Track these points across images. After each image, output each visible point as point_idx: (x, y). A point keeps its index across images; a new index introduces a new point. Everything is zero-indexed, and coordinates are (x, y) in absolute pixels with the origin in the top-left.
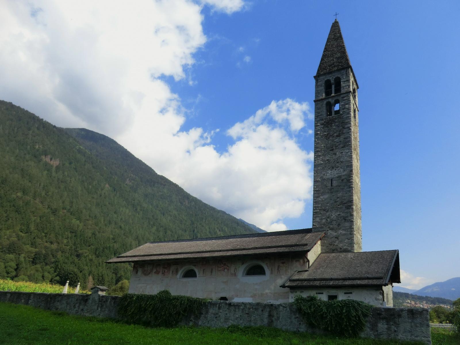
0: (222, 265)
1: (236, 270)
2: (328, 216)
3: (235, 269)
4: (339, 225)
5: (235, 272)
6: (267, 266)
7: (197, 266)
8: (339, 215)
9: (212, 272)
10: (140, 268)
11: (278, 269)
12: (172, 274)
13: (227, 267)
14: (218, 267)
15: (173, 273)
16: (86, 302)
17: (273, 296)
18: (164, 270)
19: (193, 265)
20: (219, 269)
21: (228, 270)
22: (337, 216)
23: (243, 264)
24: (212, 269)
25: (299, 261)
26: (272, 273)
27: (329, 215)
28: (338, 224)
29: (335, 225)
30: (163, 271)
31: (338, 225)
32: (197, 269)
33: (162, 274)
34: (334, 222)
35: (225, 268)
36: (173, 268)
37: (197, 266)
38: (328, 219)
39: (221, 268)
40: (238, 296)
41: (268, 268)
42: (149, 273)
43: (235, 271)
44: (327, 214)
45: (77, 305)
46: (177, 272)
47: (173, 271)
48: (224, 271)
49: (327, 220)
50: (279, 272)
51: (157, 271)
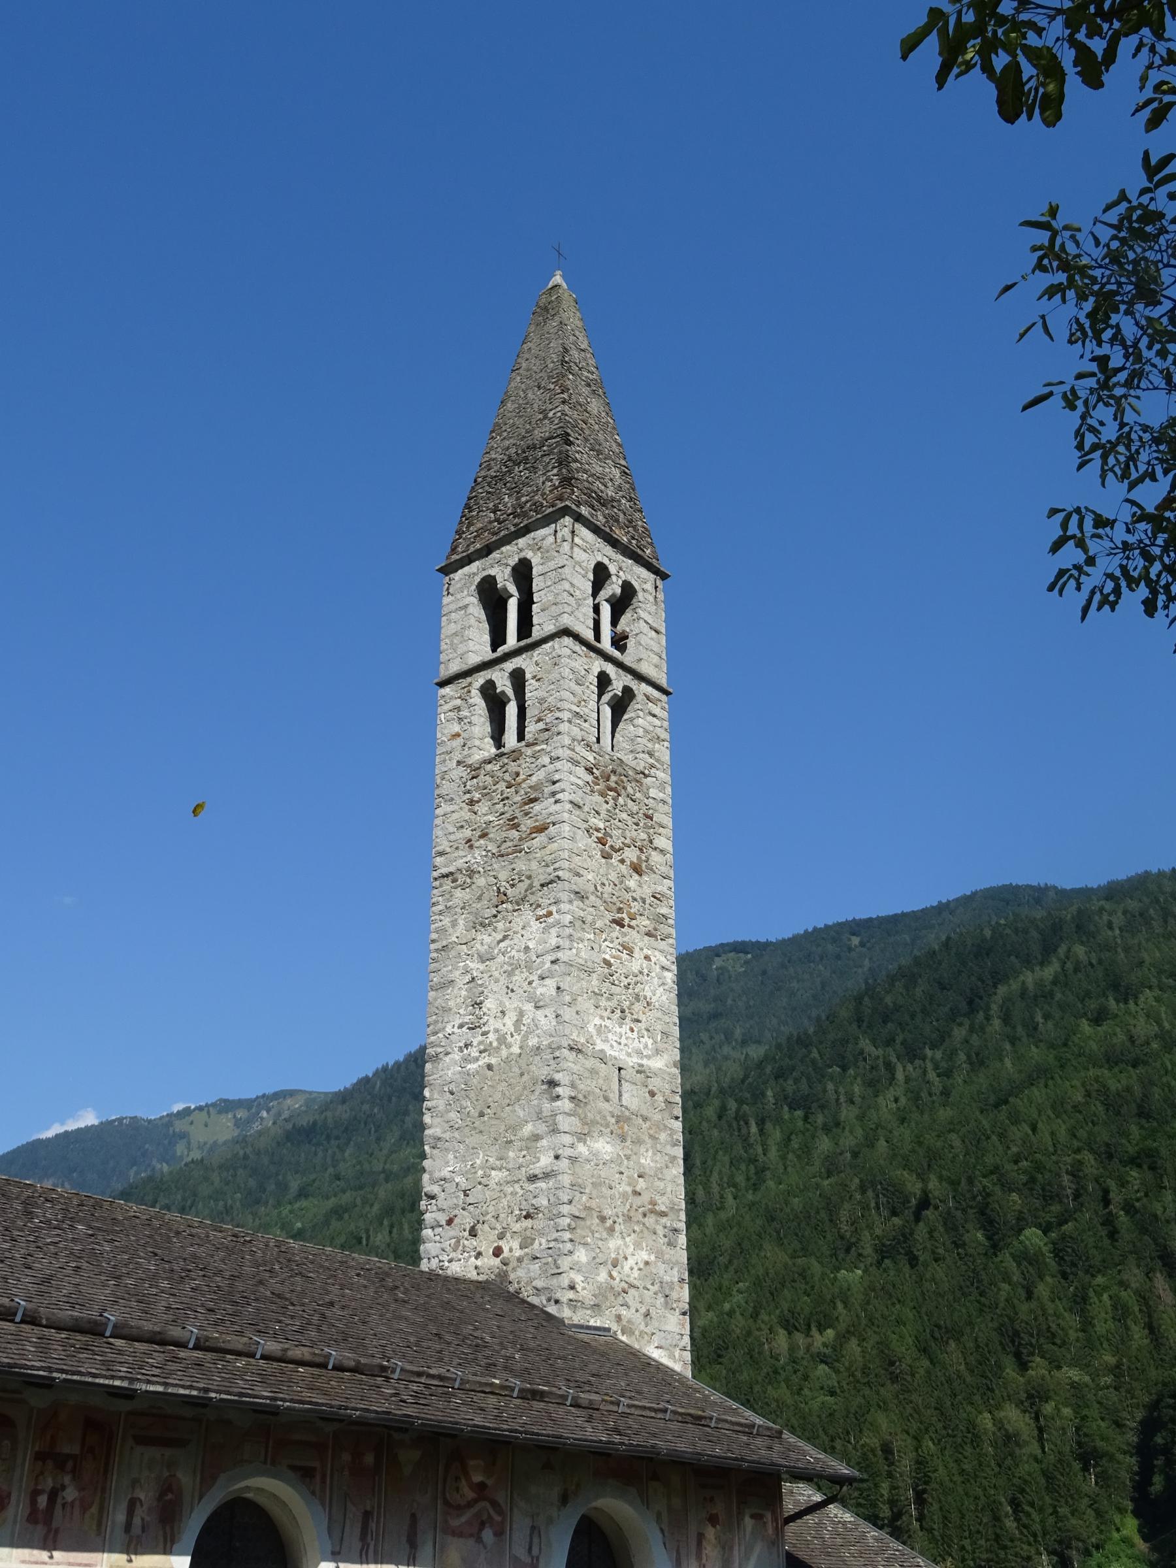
1: (536, 1540)
3: (533, 1528)
6: (662, 1531)
19: (293, 1468)
21: (499, 1534)
22: (640, 1269)
23: (564, 1499)
32: (323, 1505)
39: (463, 1519)
44: (614, 1243)
48: (479, 1540)
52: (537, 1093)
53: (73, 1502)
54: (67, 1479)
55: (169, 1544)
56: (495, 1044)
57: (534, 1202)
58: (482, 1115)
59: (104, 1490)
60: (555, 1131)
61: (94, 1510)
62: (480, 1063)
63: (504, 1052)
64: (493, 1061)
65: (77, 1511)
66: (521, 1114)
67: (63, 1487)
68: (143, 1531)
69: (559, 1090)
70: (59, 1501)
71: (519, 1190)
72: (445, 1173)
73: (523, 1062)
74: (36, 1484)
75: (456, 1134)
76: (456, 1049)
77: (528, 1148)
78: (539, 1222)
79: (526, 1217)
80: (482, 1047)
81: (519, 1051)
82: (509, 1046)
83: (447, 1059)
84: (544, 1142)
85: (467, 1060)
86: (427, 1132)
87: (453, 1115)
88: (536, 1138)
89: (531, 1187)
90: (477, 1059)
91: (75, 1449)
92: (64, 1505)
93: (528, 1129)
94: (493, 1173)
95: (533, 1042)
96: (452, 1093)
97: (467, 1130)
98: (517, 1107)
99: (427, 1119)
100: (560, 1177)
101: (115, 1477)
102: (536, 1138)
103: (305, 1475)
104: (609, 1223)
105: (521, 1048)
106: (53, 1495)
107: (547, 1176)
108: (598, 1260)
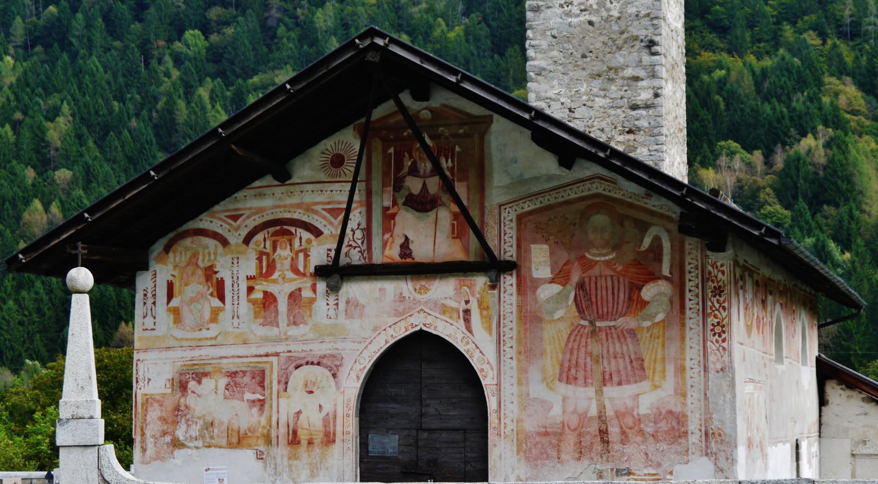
52: (636, 48)
56: (595, 7)
57: (636, 123)
58: (584, 56)
60: (653, 75)
62: (582, 18)
63: (604, 14)
64: (594, 19)
66: (621, 60)
69: (656, 48)
71: (621, 113)
72: (551, 94)
73: (622, 23)
75: (560, 68)
76: (557, 5)
77: (628, 85)
78: (640, 137)
79: (628, 132)
80: (583, 7)
81: (617, 15)
82: (609, 10)
83: (549, 11)
84: (643, 83)
85: (569, 14)
86: (528, 63)
87: (555, 53)
88: (637, 79)
89: (634, 113)
90: (578, 16)
93: (629, 72)
94: (597, 99)
95: (632, 10)
96: (554, 37)
97: (570, 66)
98: (617, 55)
99: (530, 53)
100: (659, 109)
102: (637, 79)
105: (621, 13)
107: (647, 107)
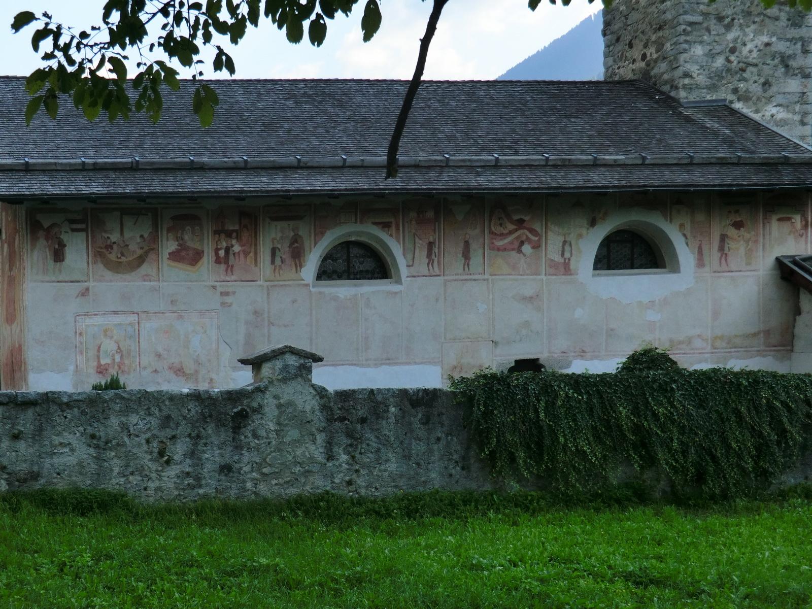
0: (511, 227)
2: (731, 45)
3: (565, 242)
4: (766, 84)
5: (567, 255)
7: (398, 229)
8: (767, 45)
9: (466, 255)
10: (73, 230)
11: (721, 249)
12: (273, 262)
13: (530, 235)
14: (491, 233)
15: (278, 261)
16: (236, 429)
17: (709, 349)
18: (224, 244)
19: (374, 223)
20: (500, 243)
21: (537, 247)
22: (759, 50)
24: (467, 244)
25: (789, 219)
26: (701, 263)
27: (735, 40)
28: (762, 80)
29: (755, 82)
30: (217, 251)
31: (764, 84)
32: (399, 242)
33: (218, 261)
34: (750, 72)
35: (524, 238)
36: (272, 235)
37: (398, 229)
38: (732, 58)
39: (506, 241)
40: (584, 351)
41: (687, 244)
42: (141, 260)
43: (563, 255)
44: (730, 36)
45: (179, 450)
46: (298, 256)
47: (274, 252)
49: (728, 60)
50: (726, 260)
51: (183, 247)
53: (239, 252)
54: (234, 242)
55: (298, 268)
59: (256, 245)
61: (252, 255)
65: (242, 256)
67: (232, 246)
68: (282, 262)
70: (231, 252)
74: (217, 245)
91: (237, 227)
92: (234, 254)
101: (261, 239)
103: (386, 226)
104: (727, 21)
106: (227, 250)
108: (714, 51)
